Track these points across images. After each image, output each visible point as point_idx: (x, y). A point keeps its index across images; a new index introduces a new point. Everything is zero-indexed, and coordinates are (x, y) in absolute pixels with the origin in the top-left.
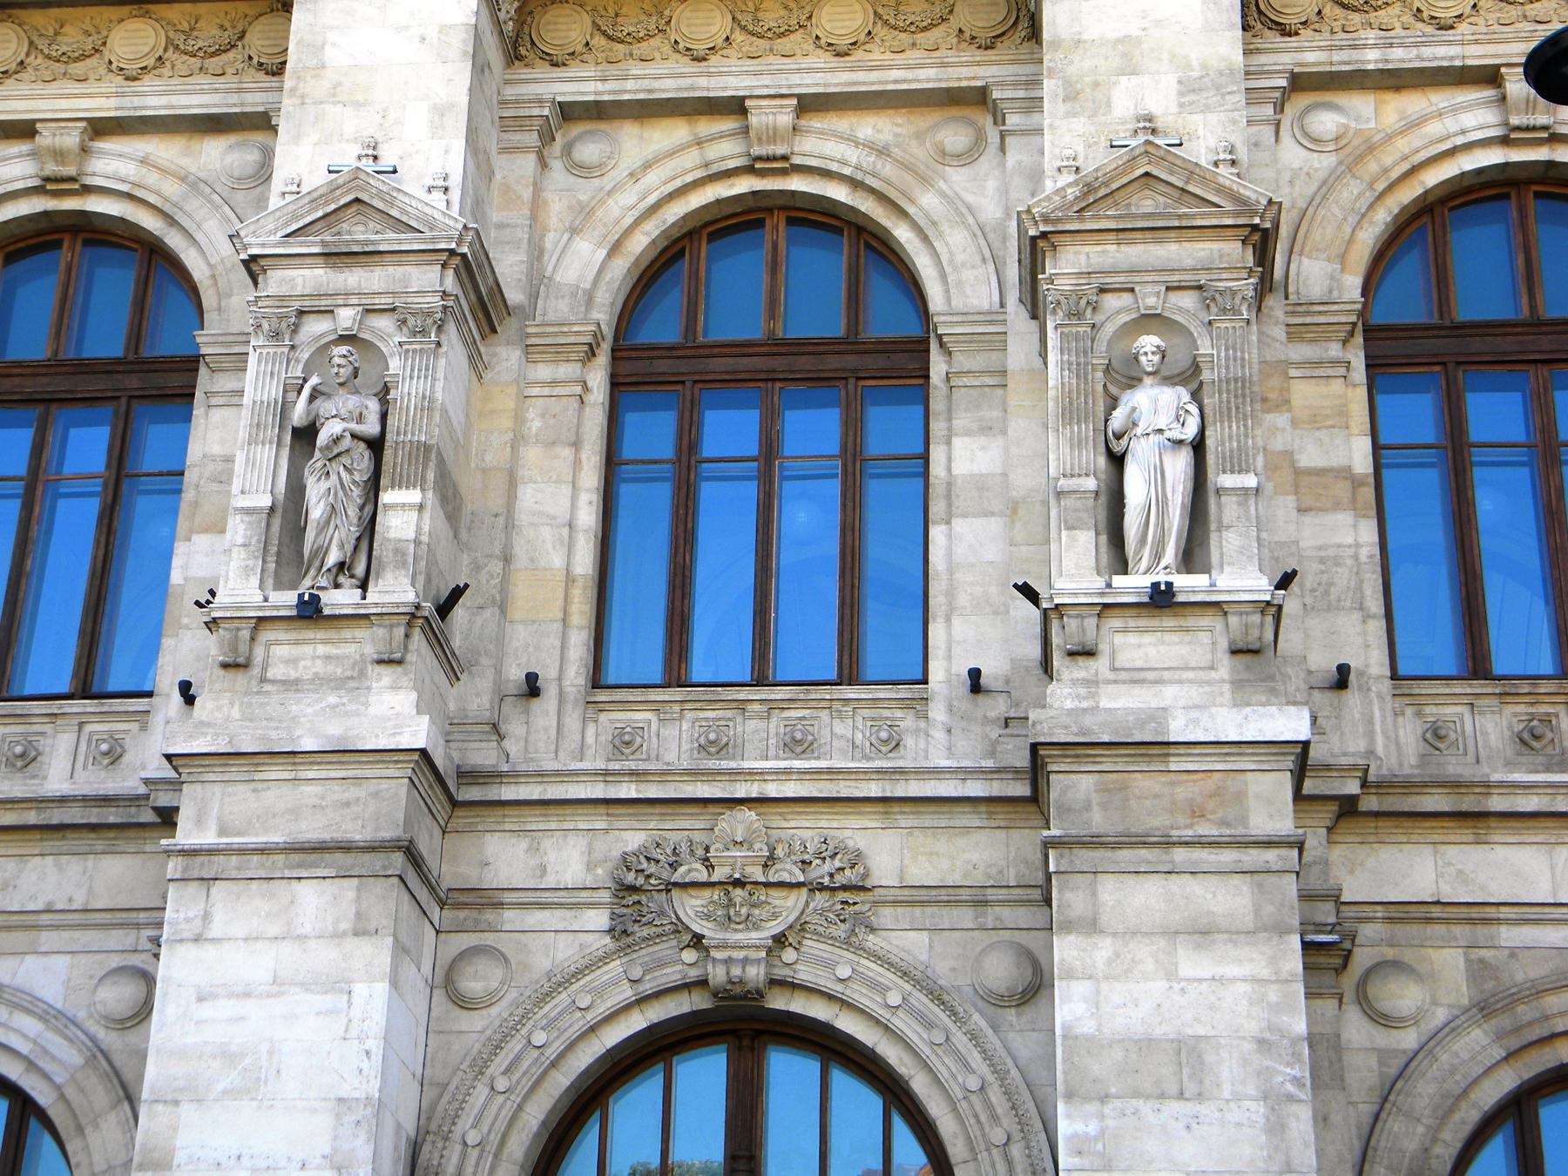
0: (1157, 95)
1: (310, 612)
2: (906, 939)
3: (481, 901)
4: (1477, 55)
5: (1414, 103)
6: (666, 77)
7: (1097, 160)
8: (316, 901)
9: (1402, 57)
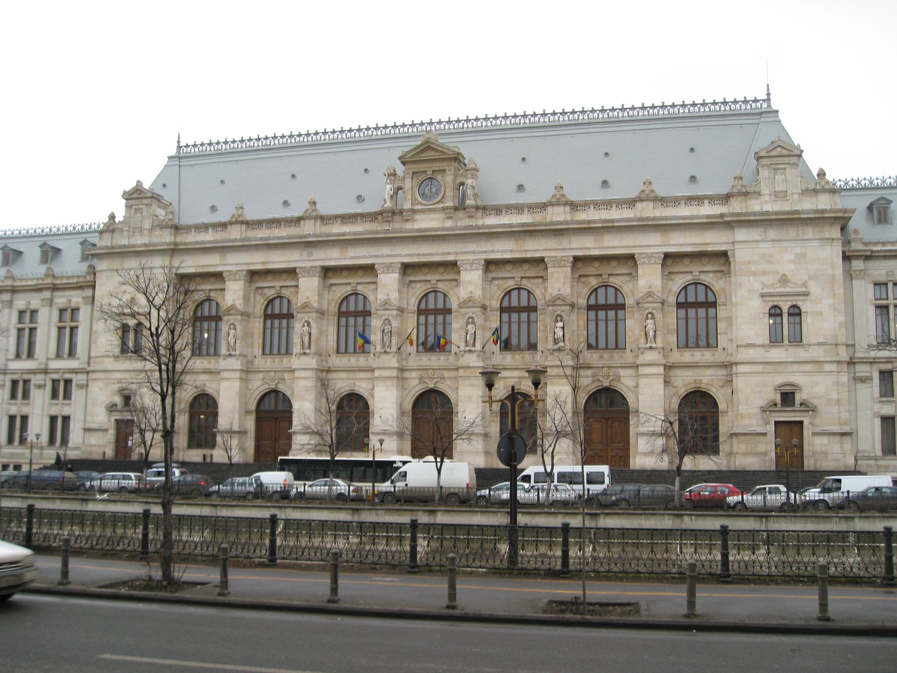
0: (471, 288)
1: (385, 352)
2: (448, 382)
3: (406, 379)
4: (512, 276)
5: (505, 281)
6: (422, 278)
7: (466, 297)
9: (504, 276)
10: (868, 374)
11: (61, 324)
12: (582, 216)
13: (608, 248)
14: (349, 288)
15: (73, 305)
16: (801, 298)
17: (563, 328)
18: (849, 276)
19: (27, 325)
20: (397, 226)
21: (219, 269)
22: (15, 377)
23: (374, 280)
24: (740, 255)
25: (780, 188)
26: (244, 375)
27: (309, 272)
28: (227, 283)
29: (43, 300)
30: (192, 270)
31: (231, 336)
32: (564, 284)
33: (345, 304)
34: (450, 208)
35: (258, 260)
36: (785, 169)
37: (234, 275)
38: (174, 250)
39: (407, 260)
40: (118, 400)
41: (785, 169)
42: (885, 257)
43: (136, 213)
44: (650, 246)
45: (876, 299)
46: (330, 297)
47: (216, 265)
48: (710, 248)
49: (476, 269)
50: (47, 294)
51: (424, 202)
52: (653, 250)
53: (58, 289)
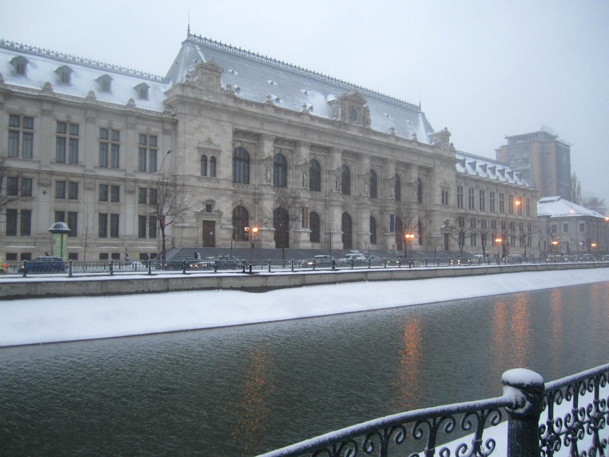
8: (339, 208)
12: (400, 143)
20: (342, 130)
21: (260, 132)
24: (437, 170)
27: (305, 144)
30: (245, 129)
37: (268, 137)
39: (345, 148)
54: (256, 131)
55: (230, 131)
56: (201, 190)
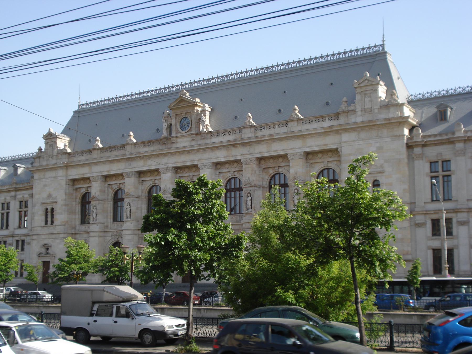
5: (226, 174)
6: (185, 175)
10: (423, 221)
11: (21, 210)
13: (274, 151)
14: (151, 183)
15: (25, 199)
16: (380, 175)
17: (251, 200)
18: (411, 159)
19: (5, 211)
21: (88, 176)
22: (17, 238)
23: (160, 178)
25: (368, 106)
26: (101, 234)
27: (129, 175)
28: (93, 183)
29: (11, 197)
31: (94, 213)
32: (251, 174)
33: (229, 184)
34: (193, 134)
35: (106, 169)
36: (370, 93)
38: (67, 167)
40: (43, 250)
41: (370, 93)
42: (436, 144)
43: (50, 147)
44: (295, 148)
45: (431, 172)
46: (143, 188)
47: (87, 174)
48: (329, 147)
49: (208, 168)
50: (13, 193)
51: (182, 132)
52: (297, 151)
53: (18, 190)
54: (85, 176)
55: (63, 183)
56: (43, 237)
